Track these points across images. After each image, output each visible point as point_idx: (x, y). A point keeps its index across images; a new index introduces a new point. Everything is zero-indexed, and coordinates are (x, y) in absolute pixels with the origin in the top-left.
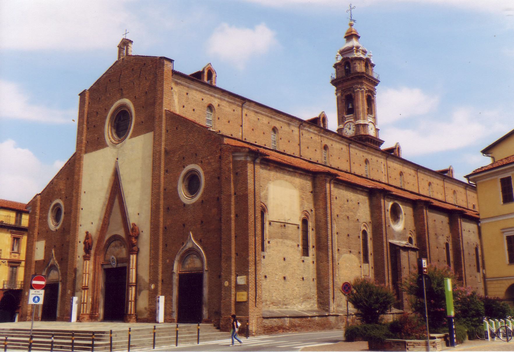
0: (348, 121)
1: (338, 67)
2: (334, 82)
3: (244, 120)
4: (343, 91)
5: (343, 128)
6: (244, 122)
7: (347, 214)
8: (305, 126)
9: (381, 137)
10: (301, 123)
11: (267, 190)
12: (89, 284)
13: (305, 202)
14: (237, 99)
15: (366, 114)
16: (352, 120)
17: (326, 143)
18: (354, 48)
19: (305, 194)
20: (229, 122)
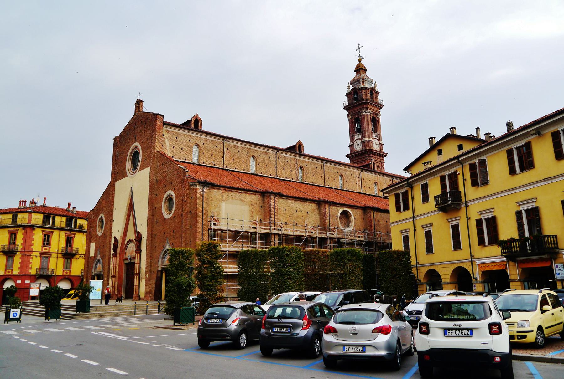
0: (357, 138)
2: (346, 108)
3: (225, 153)
4: (353, 115)
5: (353, 145)
6: (225, 154)
7: (296, 221)
10: (278, 150)
11: (220, 207)
12: (116, 273)
13: (255, 214)
14: (219, 138)
16: (360, 138)
19: (255, 209)
20: (212, 155)
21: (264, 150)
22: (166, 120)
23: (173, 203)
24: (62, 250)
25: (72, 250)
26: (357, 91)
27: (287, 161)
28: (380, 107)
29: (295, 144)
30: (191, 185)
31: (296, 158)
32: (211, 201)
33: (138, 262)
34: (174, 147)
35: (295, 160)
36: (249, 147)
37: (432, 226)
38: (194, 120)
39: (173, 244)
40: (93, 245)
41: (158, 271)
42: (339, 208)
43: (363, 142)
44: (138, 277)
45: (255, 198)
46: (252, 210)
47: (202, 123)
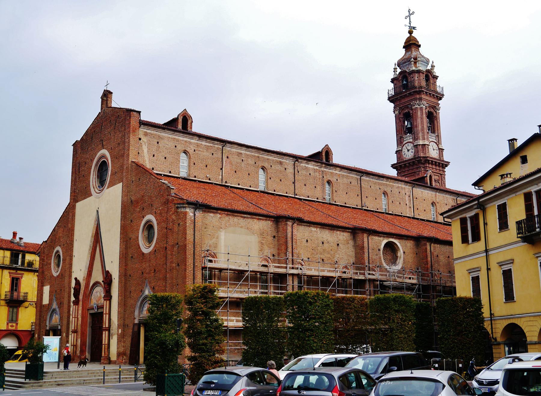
0: (406, 141)
1: (395, 82)
2: (391, 99)
3: (224, 163)
4: (401, 109)
5: (402, 150)
6: (224, 165)
7: (322, 257)
8: (301, 163)
9: (446, 159)
10: (297, 158)
11: (217, 238)
12: (78, 327)
13: (265, 247)
14: (215, 142)
15: (426, 133)
16: (411, 140)
17: (329, 179)
18: (412, 59)
19: (265, 239)
20: (206, 166)
21: (277, 159)
22: (144, 117)
23: (154, 233)
24: (6, 295)
25: (18, 296)
26: (407, 75)
27: (310, 174)
28: (440, 97)
29: (320, 150)
30: (178, 208)
31: (322, 169)
32: (206, 230)
33: (107, 312)
34: (155, 156)
35: (321, 173)
36: (256, 155)
37: (512, 263)
38: (182, 117)
39: (154, 288)
40: (47, 289)
41: (135, 324)
42: (382, 238)
43: (416, 146)
44: (107, 332)
45: (266, 225)
46: (262, 241)
47: (192, 122)
